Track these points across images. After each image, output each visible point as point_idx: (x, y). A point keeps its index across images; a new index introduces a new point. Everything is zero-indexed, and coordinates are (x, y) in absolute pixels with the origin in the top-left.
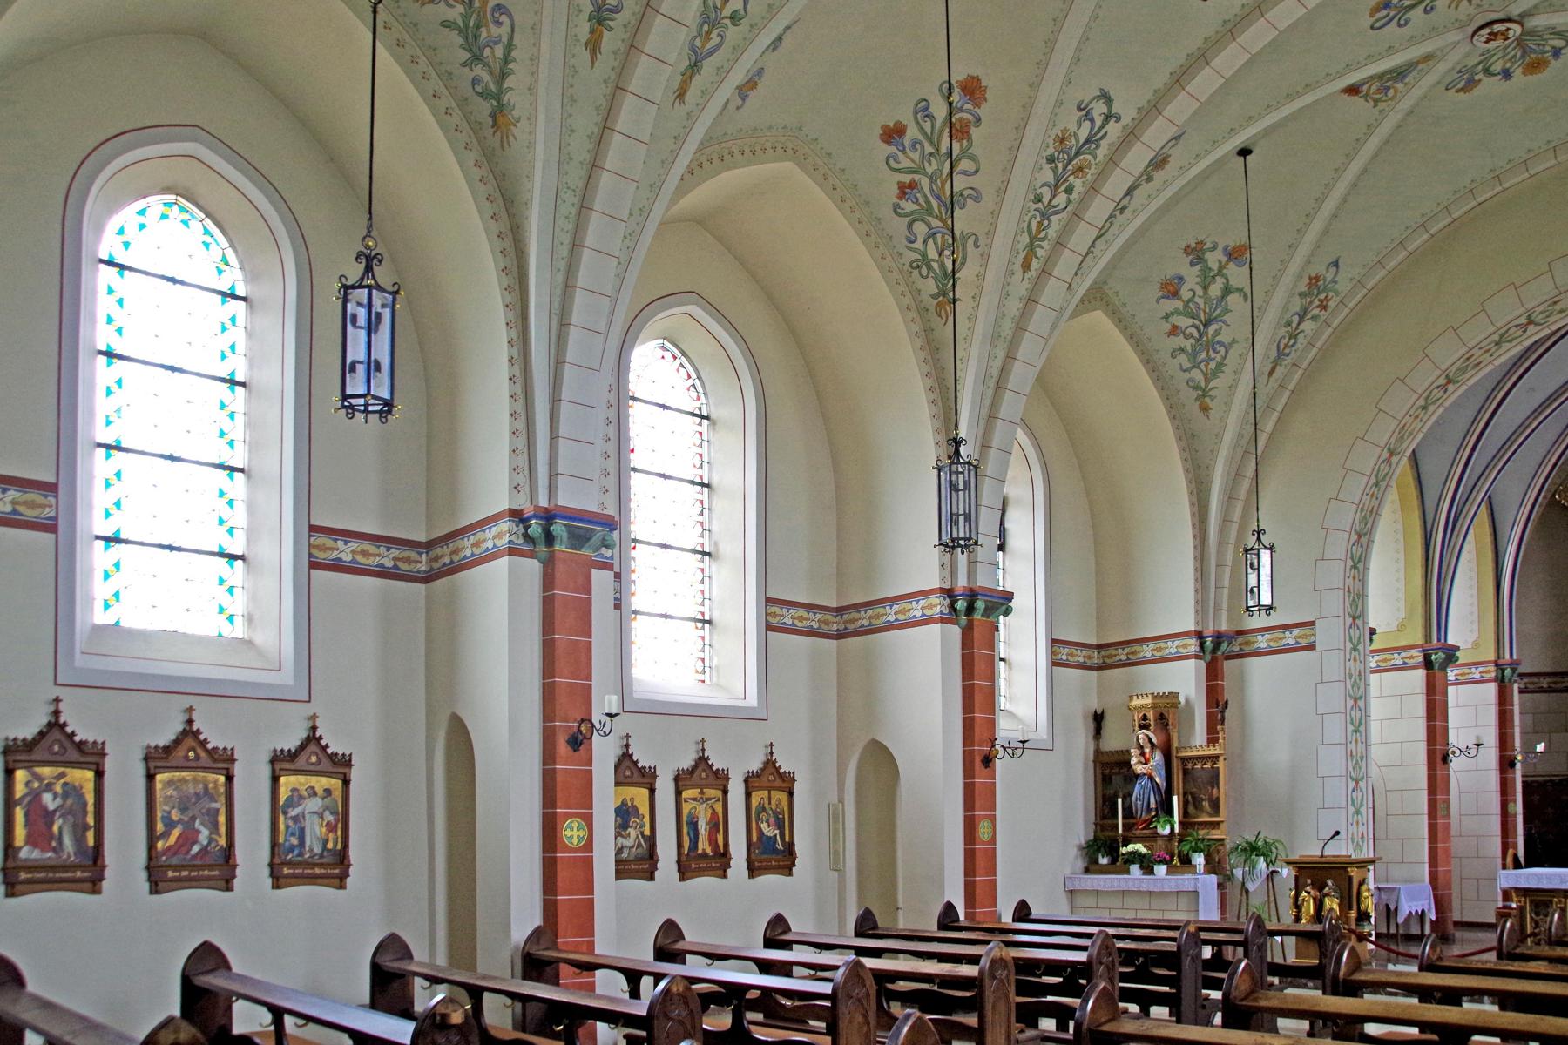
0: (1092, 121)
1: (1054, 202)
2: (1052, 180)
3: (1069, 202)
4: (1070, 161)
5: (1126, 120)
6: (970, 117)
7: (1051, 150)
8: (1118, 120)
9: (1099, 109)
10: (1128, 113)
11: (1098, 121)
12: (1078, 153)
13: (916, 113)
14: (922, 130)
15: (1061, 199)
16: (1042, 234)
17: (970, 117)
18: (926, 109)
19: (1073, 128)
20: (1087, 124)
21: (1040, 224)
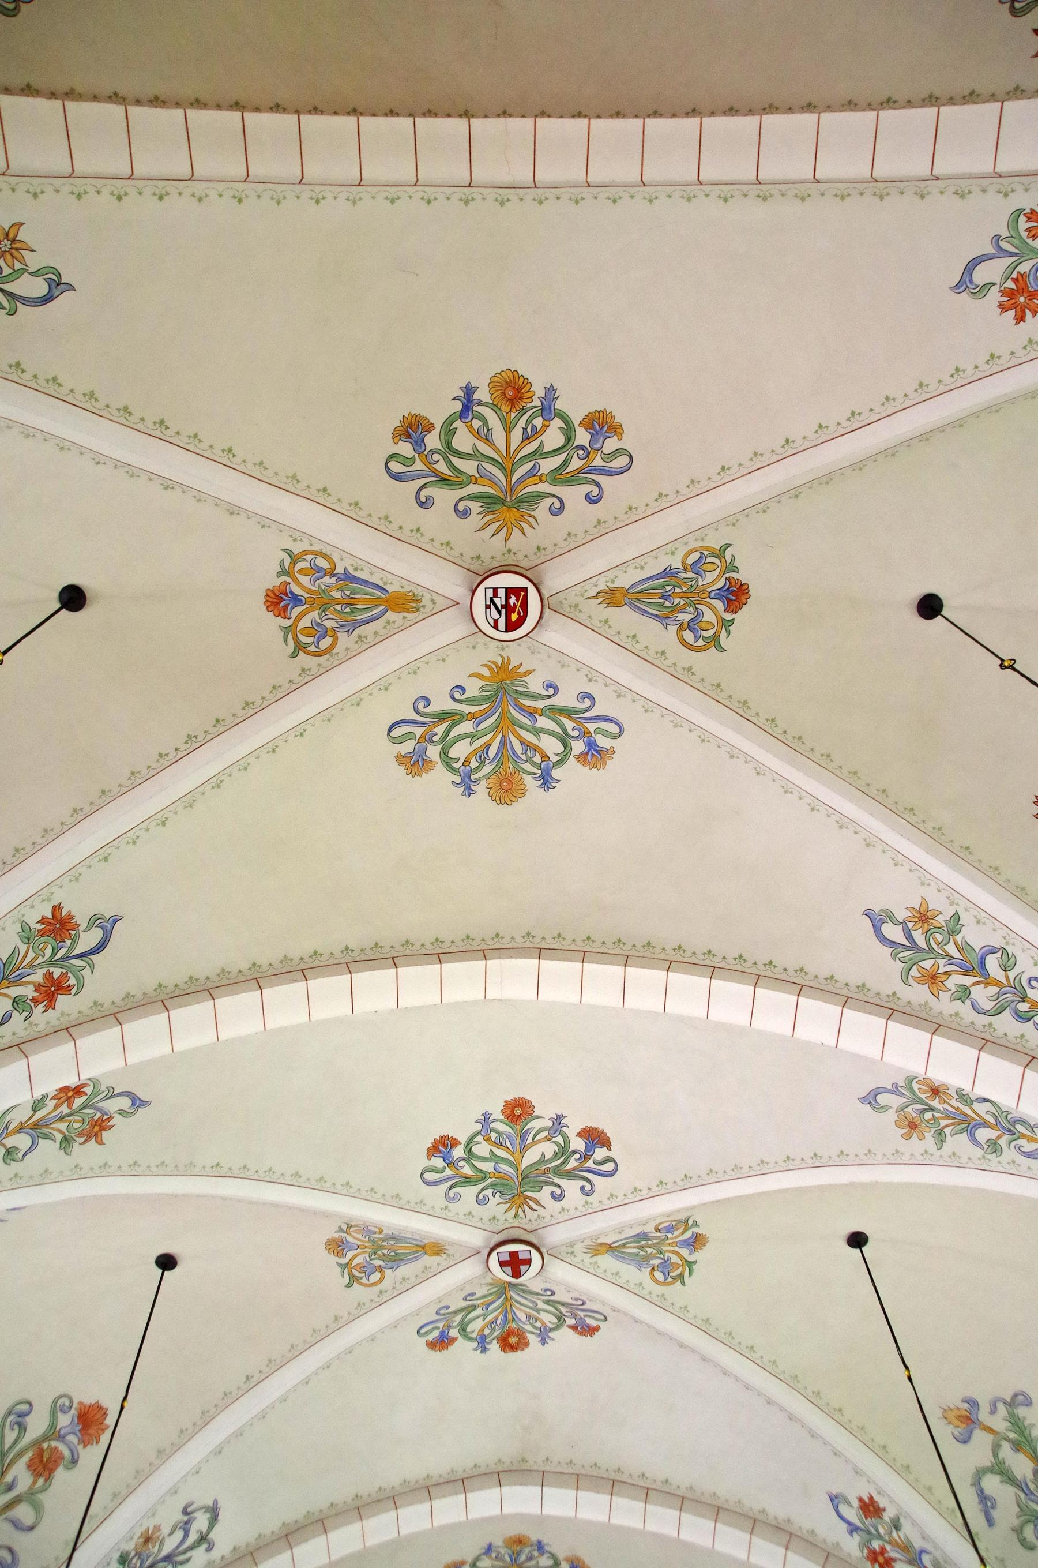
5: (216, 1554)
6: (67, 1453)
8: (209, 1549)
9: (201, 1522)
11: (193, 1537)
13: (9, 1413)
17: (67, 1453)
18: (22, 1415)
19: (165, 1530)
20: (179, 1535)
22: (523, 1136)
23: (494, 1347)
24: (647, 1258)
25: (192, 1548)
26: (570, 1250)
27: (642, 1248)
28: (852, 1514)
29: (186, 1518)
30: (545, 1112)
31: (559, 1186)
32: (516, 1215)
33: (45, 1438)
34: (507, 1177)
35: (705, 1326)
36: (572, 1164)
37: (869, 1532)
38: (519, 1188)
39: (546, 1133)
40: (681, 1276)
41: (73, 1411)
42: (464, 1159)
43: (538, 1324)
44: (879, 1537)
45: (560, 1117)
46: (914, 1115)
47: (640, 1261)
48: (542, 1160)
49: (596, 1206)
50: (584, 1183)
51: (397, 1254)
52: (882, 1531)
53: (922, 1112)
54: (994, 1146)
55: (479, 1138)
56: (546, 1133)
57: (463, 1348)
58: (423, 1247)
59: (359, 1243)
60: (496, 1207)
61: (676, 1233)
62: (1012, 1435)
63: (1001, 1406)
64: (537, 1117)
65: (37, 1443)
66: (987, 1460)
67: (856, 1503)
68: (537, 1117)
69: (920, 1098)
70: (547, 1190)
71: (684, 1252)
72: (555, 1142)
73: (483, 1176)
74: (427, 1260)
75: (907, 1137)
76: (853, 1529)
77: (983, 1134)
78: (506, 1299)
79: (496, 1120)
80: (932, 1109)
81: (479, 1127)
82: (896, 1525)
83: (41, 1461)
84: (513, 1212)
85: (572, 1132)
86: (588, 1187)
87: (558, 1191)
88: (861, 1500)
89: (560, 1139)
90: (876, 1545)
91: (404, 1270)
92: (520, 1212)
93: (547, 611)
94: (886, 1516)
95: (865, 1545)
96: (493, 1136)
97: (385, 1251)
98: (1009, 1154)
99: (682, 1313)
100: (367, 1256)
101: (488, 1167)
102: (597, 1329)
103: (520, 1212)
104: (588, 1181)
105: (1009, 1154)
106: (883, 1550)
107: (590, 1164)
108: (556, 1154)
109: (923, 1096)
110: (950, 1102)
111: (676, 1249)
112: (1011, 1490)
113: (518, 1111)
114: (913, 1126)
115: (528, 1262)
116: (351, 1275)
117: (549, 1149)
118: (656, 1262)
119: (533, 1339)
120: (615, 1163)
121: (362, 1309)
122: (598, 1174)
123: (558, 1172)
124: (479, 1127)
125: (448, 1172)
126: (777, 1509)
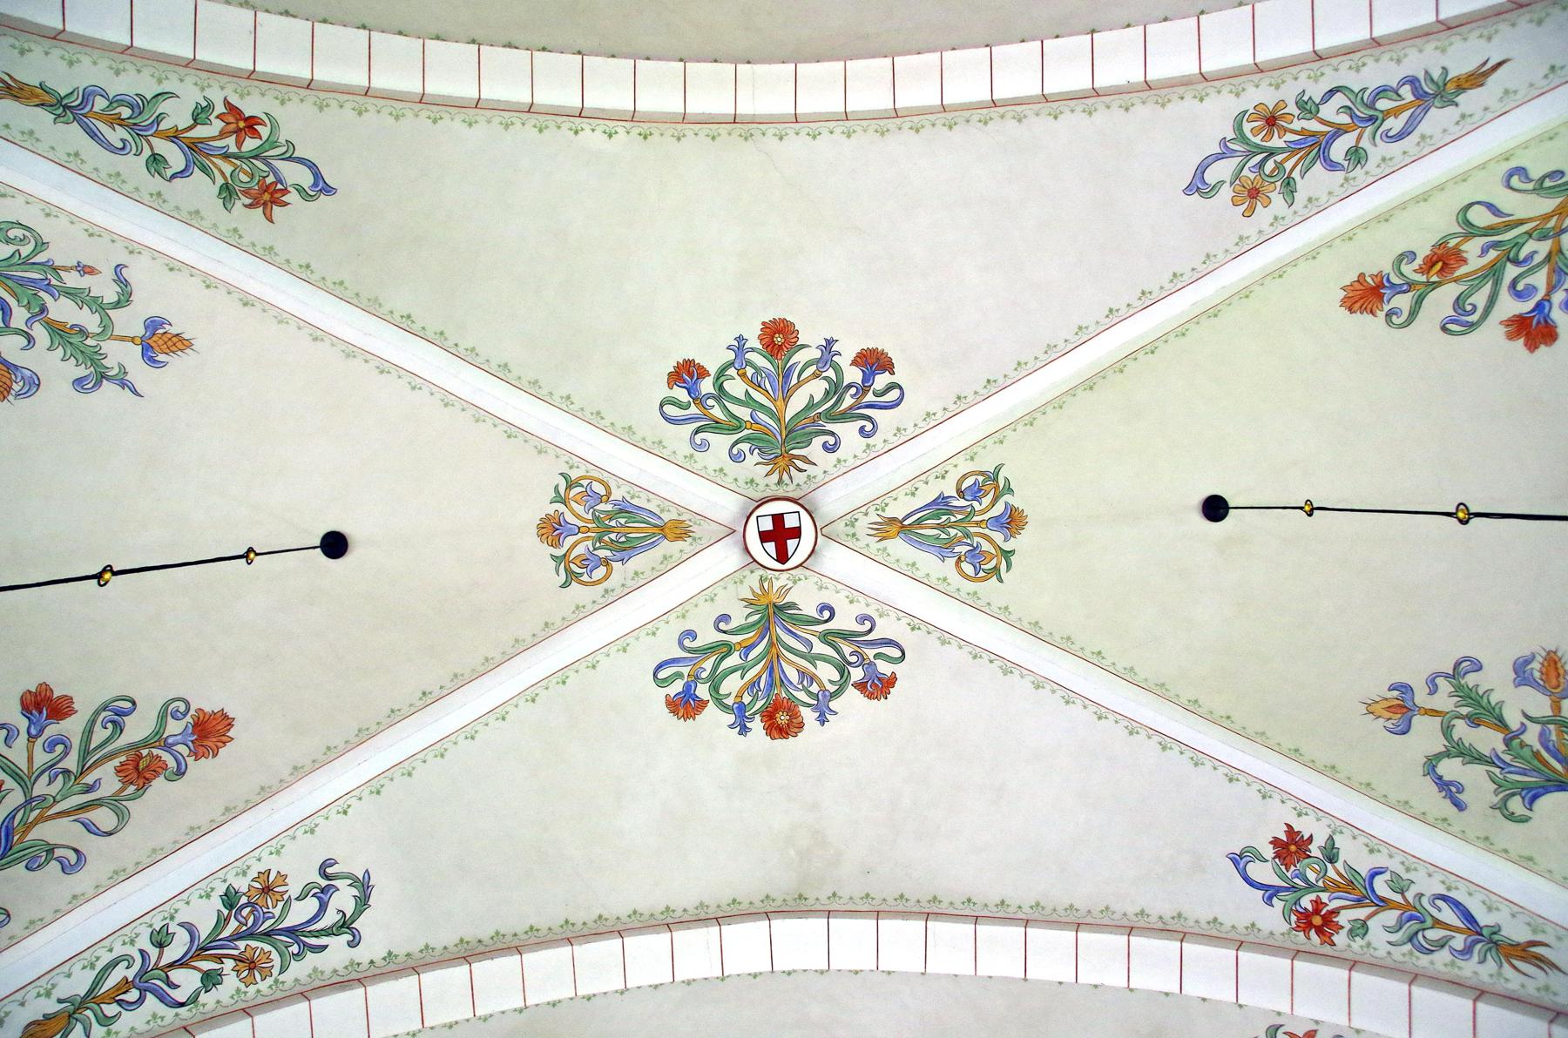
0: (323, 907)
1: (176, 975)
2: (204, 931)
3: (194, 999)
4: (250, 935)
5: (363, 954)
7: (242, 884)
8: (353, 944)
9: (344, 898)
10: (372, 948)
11: (331, 918)
12: (268, 934)
14: (89, 732)
15: (187, 981)
16: (111, 1010)
17: (172, 763)
18: (122, 713)
20: (312, 905)
21: (126, 985)
22: (787, 376)
23: (757, 725)
24: (949, 544)
25: (328, 932)
26: (850, 530)
27: (941, 527)
28: (1265, 872)
29: (324, 883)
30: (810, 337)
31: (833, 434)
32: (780, 482)
33: (145, 743)
34: (767, 431)
35: (1034, 631)
36: (848, 401)
37: (1293, 888)
38: (783, 445)
39: (813, 368)
40: (996, 569)
41: (188, 719)
42: (714, 397)
43: (814, 688)
44: (1311, 887)
45: (830, 342)
46: (1252, 176)
47: (944, 548)
48: (811, 405)
49: (880, 447)
50: (863, 423)
51: (629, 540)
52: (1312, 876)
53: (1265, 160)
54: (1357, 155)
55: (732, 372)
56: (813, 368)
57: (714, 719)
58: (662, 528)
59: (580, 524)
60: (753, 466)
61: (986, 501)
62: (1465, 711)
63: (1440, 681)
64: (803, 346)
65: (135, 747)
66: (1439, 745)
67: (1269, 852)
68: (803, 346)
69: (1257, 146)
70: (818, 441)
71: (998, 537)
72: (825, 378)
73: (734, 425)
74: (666, 547)
75: (1249, 213)
76: (1270, 893)
77: (1338, 150)
78: (771, 644)
79: (753, 350)
80: (1272, 153)
81: (732, 355)
82: (1331, 855)
83: (137, 768)
84: (775, 477)
85: (844, 361)
86: (869, 427)
87: (831, 440)
88: (1276, 842)
89: (831, 373)
90: (1306, 902)
91: (639, 562)
92: (785, 477)
93: (820, 537)
94: (1314, 850)
95: (1292, 908)
96: (750, 371)
97: (613, 536)
98: (1377, 151)
99: (1002, 615)
100: (589, 543)
101: (743, 413)
102: (891, 682)
103: (785, 477)
104: (869, 418)
105: (1377, 151)
106: (1318, 903)
107: (870, 397)
108: (827, 393)
109: (1257, 140)
110: (1291, 126)
111: (987, 531)
112: (1480, 770)
113: (779, 337)
114: (1254, 193)
115: (796, 533)
116: (569, 572)
117: (817, 388)
118: (963, 549)
119: (808, 716)
120: (901, 388)
121: (581, 613)
122: (881, 408)
123: (833, 416)
124: (732, 355)
125: (694, 410)
126: (1160, 906)
